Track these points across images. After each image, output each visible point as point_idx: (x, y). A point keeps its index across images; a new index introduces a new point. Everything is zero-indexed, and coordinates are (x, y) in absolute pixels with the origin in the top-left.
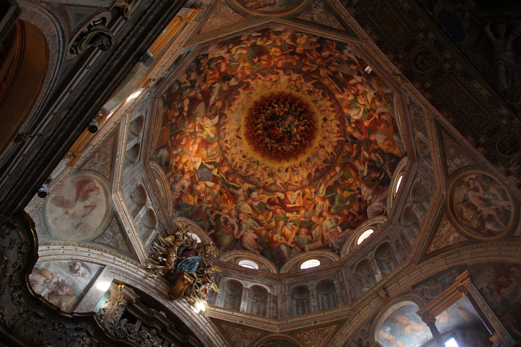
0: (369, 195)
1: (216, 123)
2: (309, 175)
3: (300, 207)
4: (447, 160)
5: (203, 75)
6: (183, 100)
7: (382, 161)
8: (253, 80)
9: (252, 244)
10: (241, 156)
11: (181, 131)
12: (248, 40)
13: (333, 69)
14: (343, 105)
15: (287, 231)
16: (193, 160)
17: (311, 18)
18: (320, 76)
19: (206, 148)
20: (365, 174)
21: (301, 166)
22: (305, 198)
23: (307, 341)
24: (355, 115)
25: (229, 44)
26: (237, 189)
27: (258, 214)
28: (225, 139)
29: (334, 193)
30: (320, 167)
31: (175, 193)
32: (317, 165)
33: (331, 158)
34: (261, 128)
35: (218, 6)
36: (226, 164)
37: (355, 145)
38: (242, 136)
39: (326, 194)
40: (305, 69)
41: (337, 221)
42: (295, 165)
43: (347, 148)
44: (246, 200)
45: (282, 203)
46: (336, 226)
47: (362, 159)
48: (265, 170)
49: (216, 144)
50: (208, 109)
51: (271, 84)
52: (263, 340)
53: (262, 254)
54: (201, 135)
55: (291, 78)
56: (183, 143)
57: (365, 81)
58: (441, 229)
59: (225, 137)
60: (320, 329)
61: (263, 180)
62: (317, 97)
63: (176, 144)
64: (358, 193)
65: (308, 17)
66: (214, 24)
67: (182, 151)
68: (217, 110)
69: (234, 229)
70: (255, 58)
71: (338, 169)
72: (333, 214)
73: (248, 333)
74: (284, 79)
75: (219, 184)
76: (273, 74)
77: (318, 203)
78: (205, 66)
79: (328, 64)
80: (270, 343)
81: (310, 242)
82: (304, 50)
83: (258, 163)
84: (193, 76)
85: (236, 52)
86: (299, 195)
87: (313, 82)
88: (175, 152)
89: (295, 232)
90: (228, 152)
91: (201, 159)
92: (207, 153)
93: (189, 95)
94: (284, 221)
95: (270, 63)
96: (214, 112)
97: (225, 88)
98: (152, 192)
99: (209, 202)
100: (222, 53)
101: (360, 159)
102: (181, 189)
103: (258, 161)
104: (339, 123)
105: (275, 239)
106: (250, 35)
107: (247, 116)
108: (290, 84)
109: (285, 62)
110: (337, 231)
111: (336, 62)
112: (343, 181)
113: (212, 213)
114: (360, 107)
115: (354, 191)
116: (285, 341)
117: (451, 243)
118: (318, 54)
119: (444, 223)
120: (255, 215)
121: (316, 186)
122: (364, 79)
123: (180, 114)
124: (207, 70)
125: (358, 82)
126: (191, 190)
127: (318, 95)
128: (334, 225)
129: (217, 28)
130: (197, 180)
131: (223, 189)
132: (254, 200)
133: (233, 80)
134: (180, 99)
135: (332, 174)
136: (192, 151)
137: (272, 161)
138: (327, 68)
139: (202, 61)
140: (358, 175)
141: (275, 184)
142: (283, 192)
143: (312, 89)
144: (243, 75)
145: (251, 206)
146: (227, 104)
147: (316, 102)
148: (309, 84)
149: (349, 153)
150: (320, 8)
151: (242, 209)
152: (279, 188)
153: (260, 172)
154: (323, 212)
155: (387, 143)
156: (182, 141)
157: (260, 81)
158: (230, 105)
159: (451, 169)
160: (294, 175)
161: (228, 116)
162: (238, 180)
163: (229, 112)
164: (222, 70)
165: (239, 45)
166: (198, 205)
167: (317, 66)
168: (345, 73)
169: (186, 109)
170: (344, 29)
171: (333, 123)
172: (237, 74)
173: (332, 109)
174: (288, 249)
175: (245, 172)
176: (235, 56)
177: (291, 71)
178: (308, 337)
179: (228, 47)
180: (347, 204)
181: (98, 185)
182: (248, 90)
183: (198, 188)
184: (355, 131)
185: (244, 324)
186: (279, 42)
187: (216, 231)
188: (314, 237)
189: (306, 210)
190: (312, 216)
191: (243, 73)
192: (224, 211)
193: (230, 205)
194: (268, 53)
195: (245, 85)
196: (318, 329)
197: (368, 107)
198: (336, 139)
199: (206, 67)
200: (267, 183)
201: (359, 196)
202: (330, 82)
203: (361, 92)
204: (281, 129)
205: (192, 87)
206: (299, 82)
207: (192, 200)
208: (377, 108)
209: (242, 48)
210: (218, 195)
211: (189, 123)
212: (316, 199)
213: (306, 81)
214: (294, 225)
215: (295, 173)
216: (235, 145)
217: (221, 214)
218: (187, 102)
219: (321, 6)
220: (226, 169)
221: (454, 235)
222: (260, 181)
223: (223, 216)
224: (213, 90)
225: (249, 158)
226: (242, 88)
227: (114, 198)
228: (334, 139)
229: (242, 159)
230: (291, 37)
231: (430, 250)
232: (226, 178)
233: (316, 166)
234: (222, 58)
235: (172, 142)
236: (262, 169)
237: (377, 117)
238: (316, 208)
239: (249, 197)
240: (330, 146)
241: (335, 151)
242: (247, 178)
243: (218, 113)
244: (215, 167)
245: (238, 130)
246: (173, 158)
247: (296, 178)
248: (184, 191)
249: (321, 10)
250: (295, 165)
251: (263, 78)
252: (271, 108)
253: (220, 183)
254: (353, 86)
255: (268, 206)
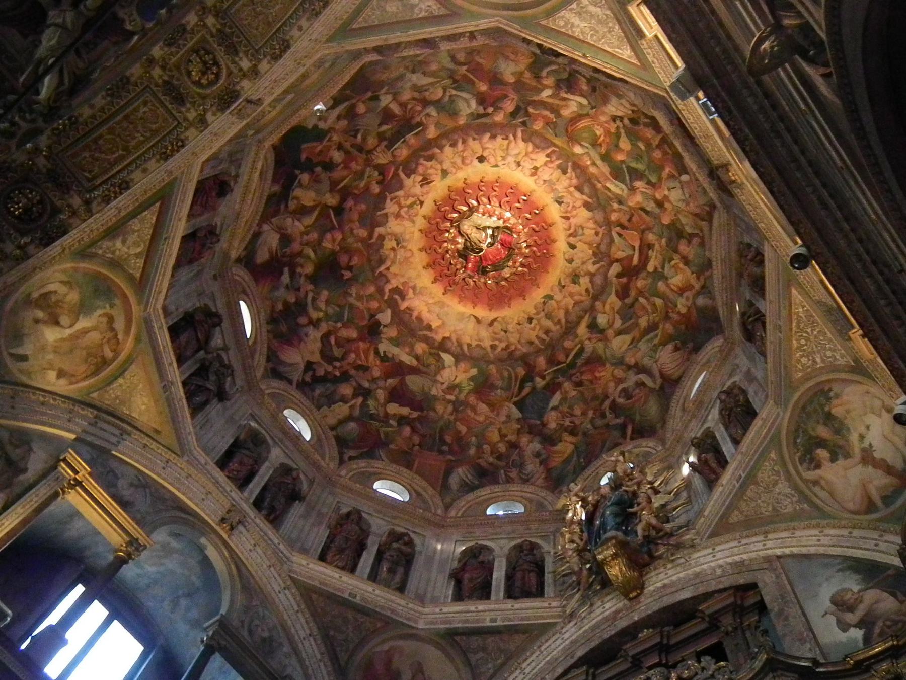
0: (622, 104)
1: (453, 359)
2: (587, 205)
3: (641, 239)
4: (415, 16)
5: (353, 372)
6: (387, 415)
7: (554, 67)
8: (388, 281)
9: (680, 360)
10: (528, 325)
11: (442, 429)
12: (298, 289)
13: (372, 141)
14: (450, 124)
15: (677, 280)
16: (503, 418)
17: (137, 258)
18: (391, 162)
19: (493, 387)
20: (584, 101)
21: (567, 218)
22: (626, 224)
23: (814, 361)
24: (468, 106)
25: (298, 325)
26: (582, 350)
27: (637, 325)
28: (489, 349)
29: (624, 166)
30: (575, 182)
31: (537, 476)
32: (570, 186)
33: (558, 159)
34: (482, 280)
35: (107, 402)
36: (532, 357)
37: (531, 110)
38: (493, 315)
39: (623, 181)
40: (376, 189)
41: (671, 176)
42: (566, 229)
43: (538, 126)
44: (606, 340)
45: (630, 272)
46: (680, 182)
47: (557, 102)
48: (564, 287)
49: (491, 366)
50: (424, 369)
51: (402, 250)
52: (789, 452)
53: (697, 349)
54: (466, 392)
55: (393, 213)
56: (463, 429)
57: (388, 89)
58: (579, 30)
59: (484, 349)
60: (794, 324)
61: (581, 295)
62: (436, 170)
63: (461, 443)
64: (621, 121)
65: (136, 263)
66: (143, 407)
67: (476, 436)
68: (431, 354)
69: (641, 384)
70: (343, 275)
71: (578, 150)
72: (660, 179)
73: (764, 475)
74: (393, 226)
75: (563, 383)
76: (382, 246)
77: (638, 203)
78: (335, 367)
79: (360, 149)
80: (798, 441)
81: (702, 244)
82: (331, 191)
83: (549, 297)
84: (346, 390)
85: (321, 310)
86: (620, 235)
87: (402, 176)
88: (472, 451)
89: (681, 266)
90: (513, 347)
91: (507, 404)
92: (502, 389)
93: (382, 401)
94: (659, 280)
95: (358, 251)
96: (432, 360)
97: (393, 333)
98: (490, 530)
99: (584, 413)
100: (314, 336)
101: (558, 105)
102: (537, 460)
103: (545, 297)
104: (488, 135)
105: (684, 310)
106: (287, 287)
107: (456, 300)
108: (406, 216)
109: (357, 223)
110: (687, 183)
111: (355, 136)
112: (601, 145)
113: (603, 416)
114: (451, 96)
115: (618, 128)
116: (804, 408)
117: (608, 12)
118: (340, 168)
119: (562, 23)
120: (636, 333)
121: (609, 197)
122: (384, 90)
123: (409, 424)
124: (344, 363)
125: (394, 99)
126: (549, 440)
127: (431, 167)
128: (678, 185)
129: (152, 404)
130: (538, 422)
131: (574, 378)
132: (610, 325)
133: (380, 317)
134: (379, 421)
135: (589, 163)
136: (486, 416)
137: (550, 270)
138: (370, 152)
139: (321, 372)
140: (588, 115)
141: (592, 275)
142: (610, 265)
143: (420, 178)
144: (375, 299)
145: (619, 333)
146: (425, 333)
147: (445, 173)
148: (408, 182)
149: (547, 124)
150: (114, 245)
151: (618, 354)
152: (601, 270)
153: (565, 297)
154: (655, 197)
155: (512, 57)
156: (460, 432)
157: (392, 269)
158: (429, 328)
159: (435, 7)
160: (583, 234)
161: (447, 335)
162: (568, 344)
163: (440, 331)
164: (354, 335)
165: (306, 304)
166: (580, 438)
167: (368, 169)
168: (378, 122)
169: (405, 411)
170: (158, 205)
171: (488, 145)
172: (369, 309)
173: (460, 144)
174: (704, 293)
175: (558, 327)
176: (330, 311)
177: (379, 213)
178: (808, 356)
179: (305, 326)
180: (643, 148)
181: (386, 647)
182: (408, 291)
183: (553, 425)
184: (501, 108)
185: (743, 476)
186: (310, 236)
187: (633, 421)
188: (696, 232)
189: (649, 229)
190: (660, 221)
191: (371, 297)
192: (610, 391)
193: (605, 373)
194: (333, 253)
195: (396, 297)
196: (794, 329)
197: (448, 82)
198: (521, 144)
199: (338, 364)
200: (587, 290)
201: (626, 121)
202: (403, 145)
203: (416, 95)
204: (484, 246)
205: (366, 394)
206: (402, 199)
207: (566, 447)
208: (444, 68)
209: (314, 299)
210: (580, 391)
211: (434, 410)
212: (631, 204)
213: (401, 187)
214: (670, 262)
215: (581, 231)
216: (506, 332)
217: (612, 398)
218: (393, 408)
219: (110, 244)
220: (541, 361)
221: (587, 5)
222: (582, 302)
223: (616, 395)
224: (390, 355)
225: (534, 311)
226: (399, 301)
227: (427, 624)
228: (519, 147)
229: (532, 325)
230: (298, 216)
231: (629, 57)
232: (557, 365)
233: (572, 189)
234: (325, 337)
235: (451, 452)
236: (561, 291)
237: (465, 68)
238: (648, 209)
239: (602, 332)
240: (533, 156)
241: (543, 149)
242: (569, 325)
243: (436, 351)
244: (532, 380)
245: (478, 321)
246: (479, 458)
247: (589, 233)
248: (543, 457)
249: (118, 244)
250: (566, 229)
251: (388, 263)
252: (448, 256)
253: (561, 379)
254: (406, 108)
255: (628, 301)
